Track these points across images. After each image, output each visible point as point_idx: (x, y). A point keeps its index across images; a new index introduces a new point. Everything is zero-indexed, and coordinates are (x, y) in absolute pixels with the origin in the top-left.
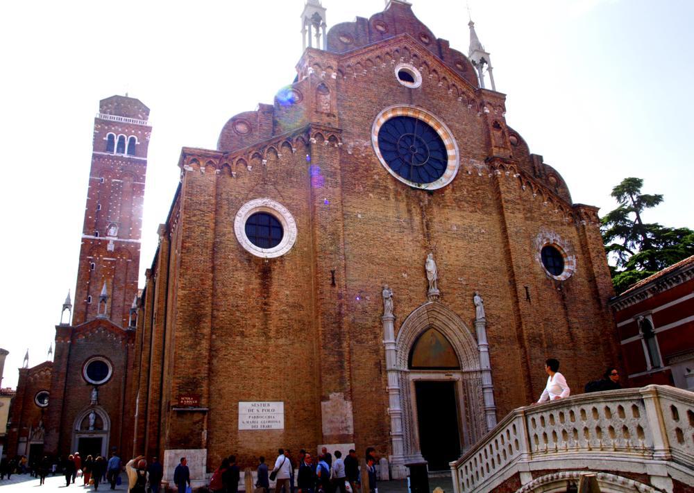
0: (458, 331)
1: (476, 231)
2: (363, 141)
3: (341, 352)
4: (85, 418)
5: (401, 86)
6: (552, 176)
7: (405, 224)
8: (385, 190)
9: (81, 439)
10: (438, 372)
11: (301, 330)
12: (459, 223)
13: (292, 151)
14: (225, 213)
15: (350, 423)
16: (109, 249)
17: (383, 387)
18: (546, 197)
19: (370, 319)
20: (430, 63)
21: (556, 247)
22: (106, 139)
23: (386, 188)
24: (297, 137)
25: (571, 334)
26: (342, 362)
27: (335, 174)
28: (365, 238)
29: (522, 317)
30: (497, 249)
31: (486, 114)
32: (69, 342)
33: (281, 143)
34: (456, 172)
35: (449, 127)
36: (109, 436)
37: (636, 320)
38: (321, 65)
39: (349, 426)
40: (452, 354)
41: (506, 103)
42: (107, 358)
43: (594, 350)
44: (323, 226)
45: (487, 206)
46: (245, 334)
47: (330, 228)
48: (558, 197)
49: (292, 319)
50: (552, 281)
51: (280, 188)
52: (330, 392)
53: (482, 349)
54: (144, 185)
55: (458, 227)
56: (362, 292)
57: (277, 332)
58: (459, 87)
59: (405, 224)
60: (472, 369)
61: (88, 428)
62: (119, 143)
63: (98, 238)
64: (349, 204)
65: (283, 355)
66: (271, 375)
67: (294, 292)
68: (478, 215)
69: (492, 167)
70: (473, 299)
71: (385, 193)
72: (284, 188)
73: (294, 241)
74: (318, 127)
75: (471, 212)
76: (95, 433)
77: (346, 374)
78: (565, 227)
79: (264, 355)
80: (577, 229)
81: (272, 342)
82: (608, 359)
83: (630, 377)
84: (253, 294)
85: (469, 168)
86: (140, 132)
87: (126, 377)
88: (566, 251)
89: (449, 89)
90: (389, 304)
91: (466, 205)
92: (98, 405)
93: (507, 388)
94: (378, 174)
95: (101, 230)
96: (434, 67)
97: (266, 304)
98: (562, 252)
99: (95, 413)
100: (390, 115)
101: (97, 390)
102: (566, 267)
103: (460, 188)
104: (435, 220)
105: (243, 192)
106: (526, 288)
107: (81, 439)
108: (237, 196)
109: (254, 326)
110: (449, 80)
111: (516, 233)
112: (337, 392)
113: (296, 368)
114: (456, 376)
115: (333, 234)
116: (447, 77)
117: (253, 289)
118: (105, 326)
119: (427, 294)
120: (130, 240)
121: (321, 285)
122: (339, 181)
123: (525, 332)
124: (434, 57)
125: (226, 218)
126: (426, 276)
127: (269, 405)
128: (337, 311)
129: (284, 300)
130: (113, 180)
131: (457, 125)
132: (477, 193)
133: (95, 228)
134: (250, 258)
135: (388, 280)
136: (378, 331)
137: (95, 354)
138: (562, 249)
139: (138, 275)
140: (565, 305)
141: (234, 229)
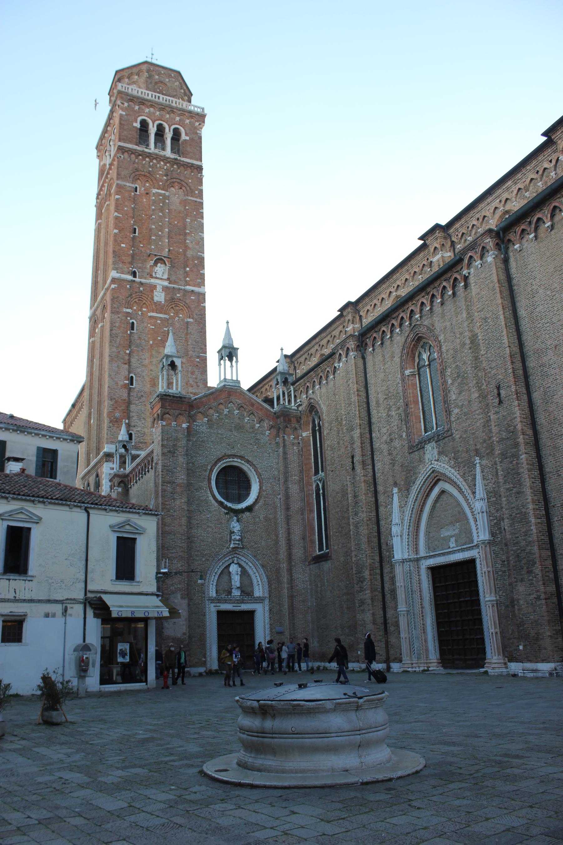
4: (222, 572)
9: (221, 614)
16: (156, 299)
22: (137, 125)
32: (184, 425)
36: (267, 608)
42: (248, 461)
54: (202, 203)
61: (230, 592)
62: (156, 134)
63: (137, 279)
76: (242, 602)
86: (187, 121)
87: (287, 497)
92: (243, 548)
95: (140, 268)
99: (240, 566)
101: (238, 521)
107: (221, 614)
118: (239, 402)
120: (188, 288)
130: (154, 191)
133: (131, 263)
137: (229, 453)
139: (206, 346)
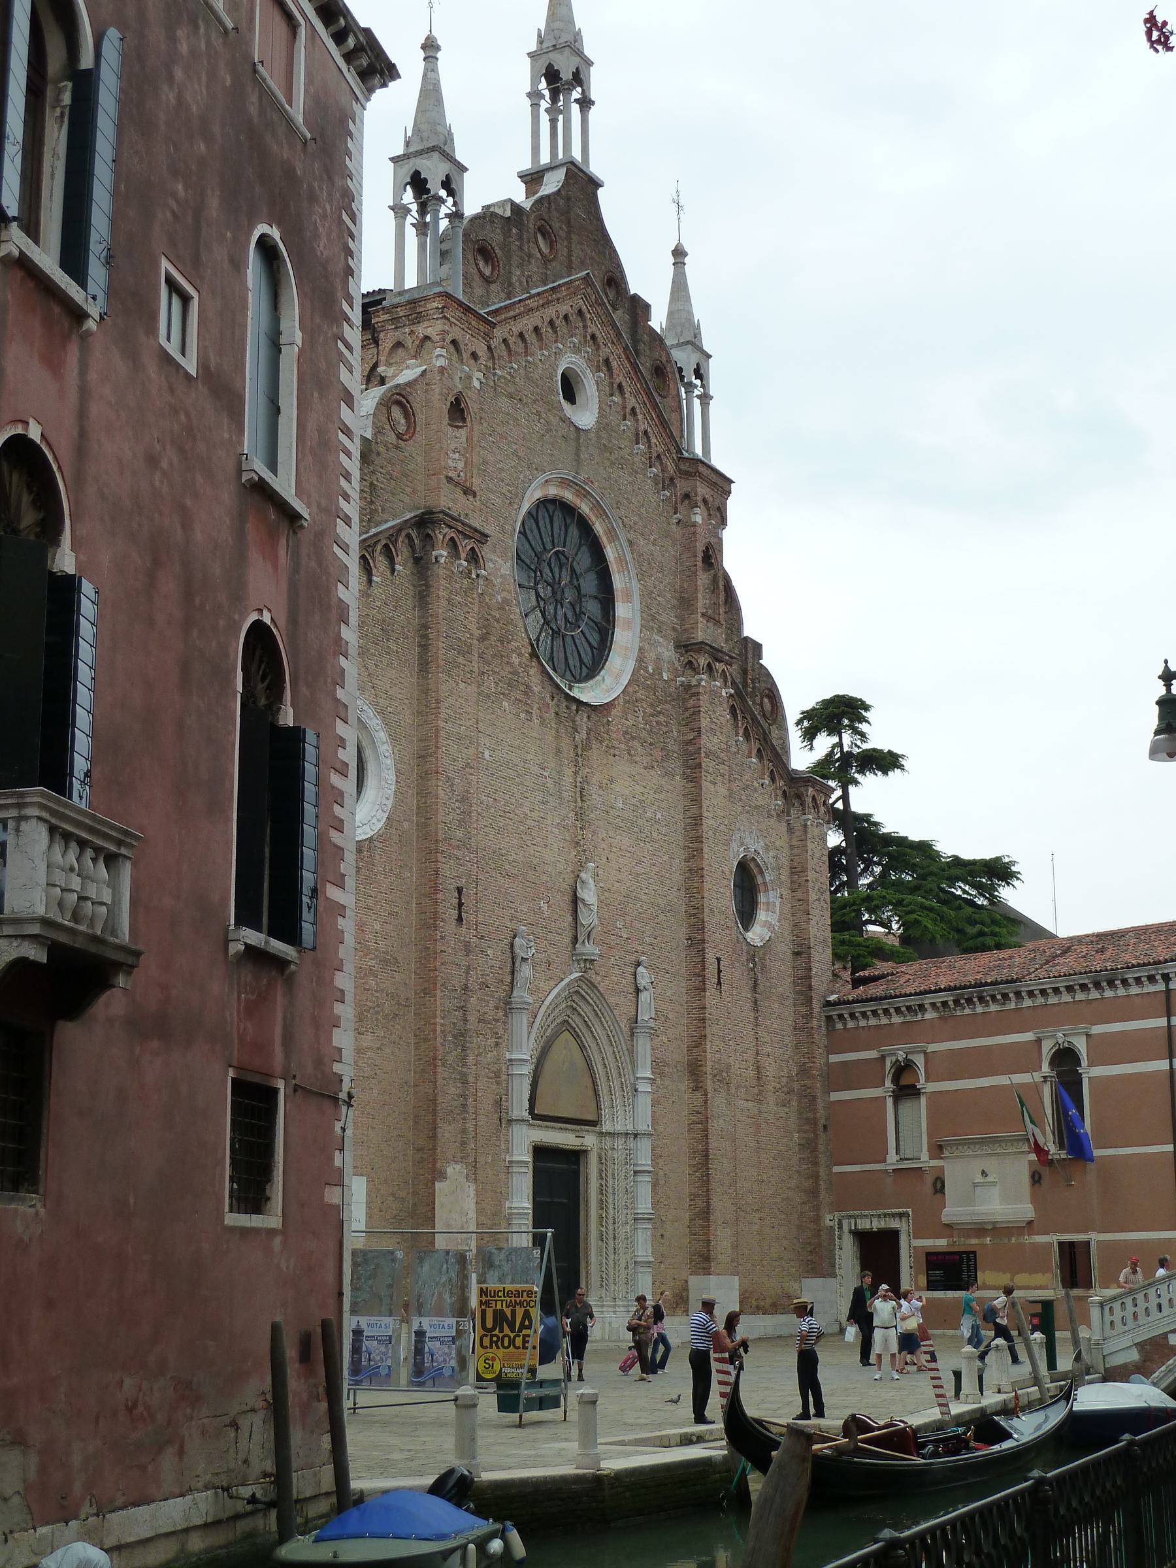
0: (604, 1039)
1: (649, 815)
2: (500, 561)
5: (565, 420)
6: (768, 696)
8: (526, 694)
10: (566, 1129)
13: (393, 570)
18: (755, 745)
19: (492, 1004)
20: (614, 364)
23: (528, 687)
25: (758, 1069)
26: (465, 1097)
28: (492, 810)
29: (708, 1022)
30: (676, 863)
31: (694, 525)
33: (379, 548)
34: (631, 665)
37: (883, 1058)
38: (462, 346)
40: (591, 1092)
41: (728, 502)
43: (785, 1106)
45: (667, 756)
49: (382, 991)
51: (371, 665)
53: (644, 1087)
58: (654, 440)
60: (619, 1128)
67: (388, 927)
68: (655, 777)
69: (690, 662)
70: (635, 975)
73: (390, 803)
75: (645, 768)
77: (470, 1126)
78: (773, 822)
80: (790, 830)
82: (807, 1127)
83: (836, 1169)
85: (651, 656)
88: (768, 879)
89: (638, 443)
90: (525, 971)
96: (621, 378)
98: (759, 880)
100: (538, 494)
102: (762, 915)
106: (719, 960)
110: (640, 417)
111: (716, 830)
112: (456, 1162)
114: (589, 1141)
115: (462, 800)
116: (638, 411)
119: (575, 956)
121: (443, 920)
123: (709, 1056)
124: (626, 349)
126: (575, 911)
132: (658, 723)
136: (501, 1031)
138: (761, 872)
140: (755, 1002)
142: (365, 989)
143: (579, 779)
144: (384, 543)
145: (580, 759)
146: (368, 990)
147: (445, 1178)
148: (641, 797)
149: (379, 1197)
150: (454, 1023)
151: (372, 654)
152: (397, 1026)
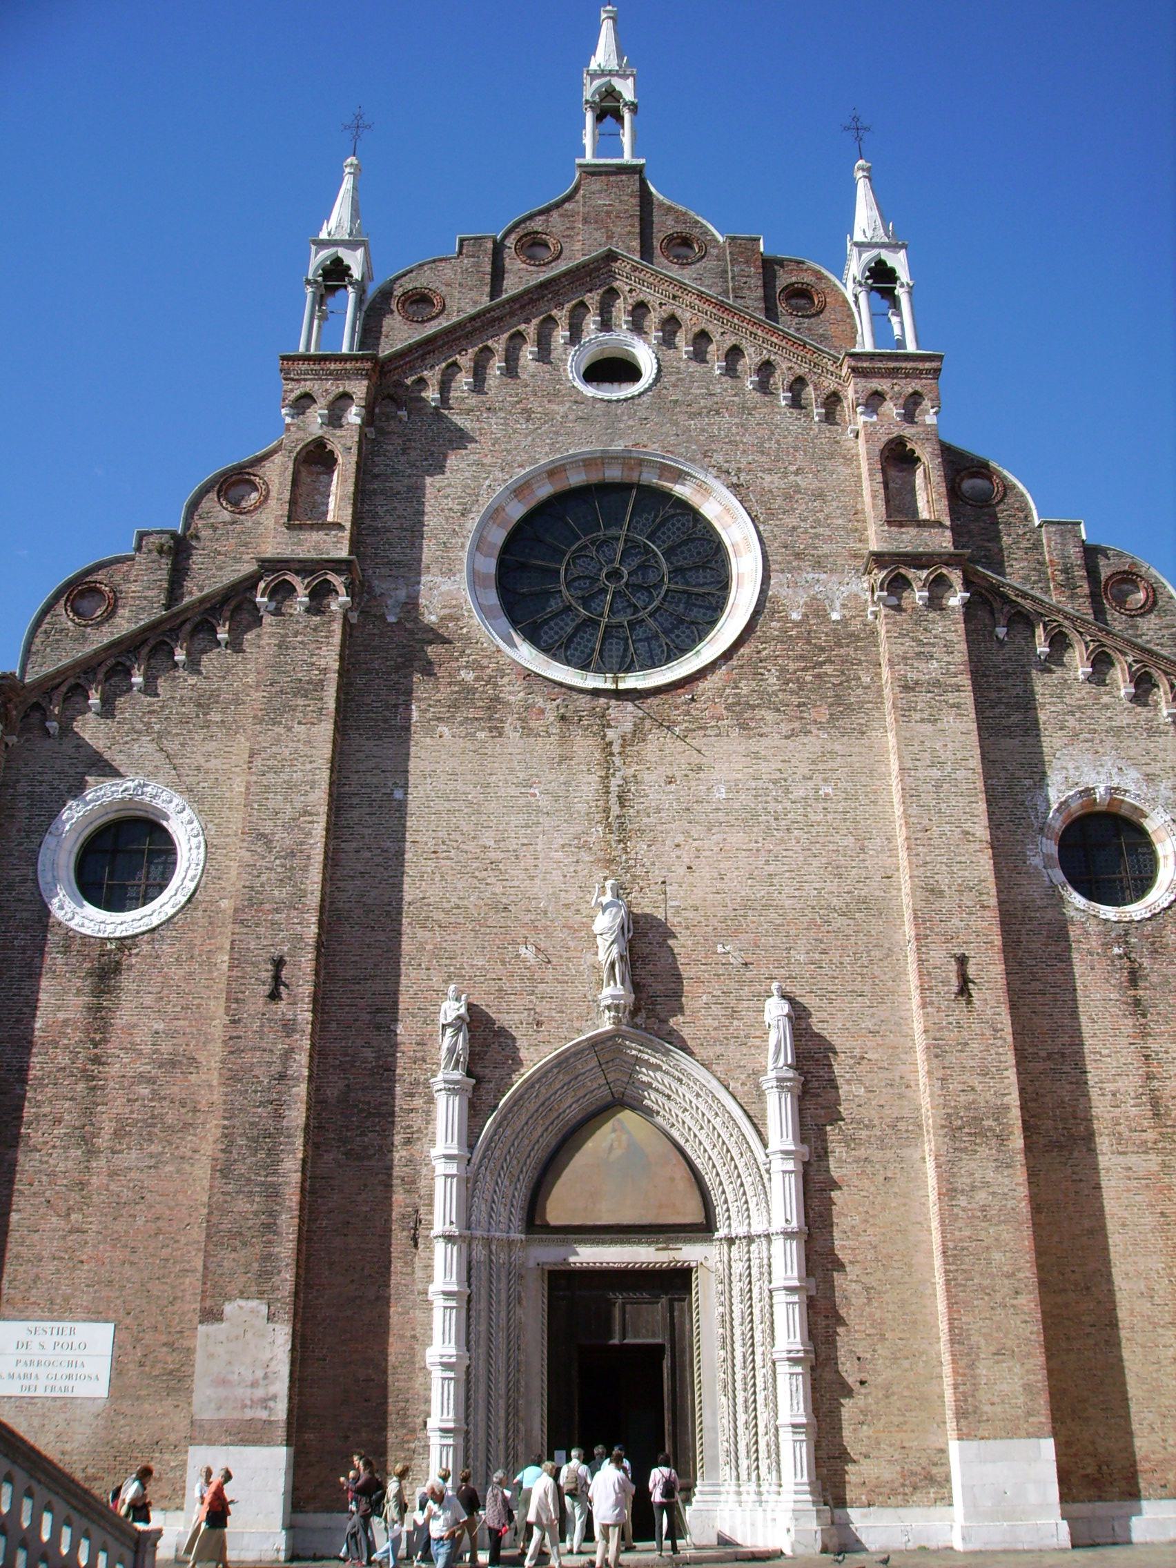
3: (272, 1184)
5: (581, 400)
7: (544, 802)
11: (186, 1126)
12: (739, 776)
14: (19, 831)
15: (281, 1387)
17: (420, 1287)
21: (1124, 811)
23: (496, 701)
24: (233, 603)
26: (273, 1214)
27: (320, 685)
33: (188, 627)
35: (735, 488)
39: (274, 1398)
44: (262, 835)
46: (31, 1143)
47: (283, 839)
48: (1135, 646)
50: (1092, 927)
51: (172, 746)
52: (228, 1298)
55: (734, 787)
56: (379, 1010)
57: (118, 1134)
59: (544, 802)
64: (371, 764)
65: (126, 1194)
66: (88, 1250)
67: (181, 1023)
68: (814, 743)
71: (490, 719)
72: (182, 745)
74: (279, 566)
75: (787, 737)
79: (75, 1197)
81: (99, 1163)
84: (65, 1035)
91: (770, 716)
93: (867, 1289)
94: (476, 666)
97: (96, 1060)
103: (755, 669)
104: (654, 777)
105: (72, 772)
106: (962, 961)
108: (56, 782)
109: (58, 1121)
113: (159, 1232)
117: (66, 1020)
121: (237, 1001)
122: (331, 705)
125: (20, 844)
127: (72, 1331)
128: (276, 1069)
129: (147, 1049)
131: (768, 478)
134: (70, 937)
135: (468, 971)
136: (417, 1121)
141: (36, 872)
142: (129, 1100)
143: (615, 782)
144: (198, 619)
145: (617, 760)
146: (136, 1100)
147: (222, 1320)
148: (778, 775)
149: (138, 1350)
150: (251, 1124)
151: (178, 734)
152: (190, 1138)
